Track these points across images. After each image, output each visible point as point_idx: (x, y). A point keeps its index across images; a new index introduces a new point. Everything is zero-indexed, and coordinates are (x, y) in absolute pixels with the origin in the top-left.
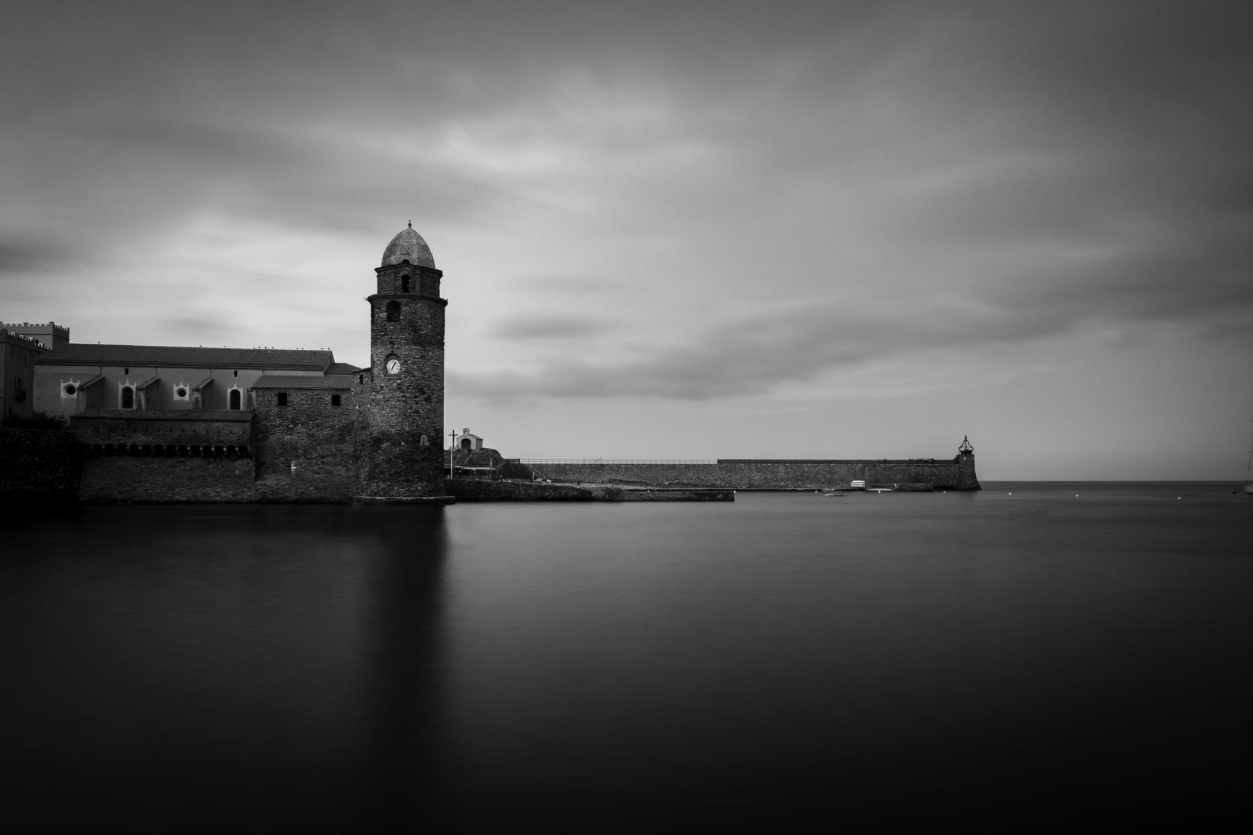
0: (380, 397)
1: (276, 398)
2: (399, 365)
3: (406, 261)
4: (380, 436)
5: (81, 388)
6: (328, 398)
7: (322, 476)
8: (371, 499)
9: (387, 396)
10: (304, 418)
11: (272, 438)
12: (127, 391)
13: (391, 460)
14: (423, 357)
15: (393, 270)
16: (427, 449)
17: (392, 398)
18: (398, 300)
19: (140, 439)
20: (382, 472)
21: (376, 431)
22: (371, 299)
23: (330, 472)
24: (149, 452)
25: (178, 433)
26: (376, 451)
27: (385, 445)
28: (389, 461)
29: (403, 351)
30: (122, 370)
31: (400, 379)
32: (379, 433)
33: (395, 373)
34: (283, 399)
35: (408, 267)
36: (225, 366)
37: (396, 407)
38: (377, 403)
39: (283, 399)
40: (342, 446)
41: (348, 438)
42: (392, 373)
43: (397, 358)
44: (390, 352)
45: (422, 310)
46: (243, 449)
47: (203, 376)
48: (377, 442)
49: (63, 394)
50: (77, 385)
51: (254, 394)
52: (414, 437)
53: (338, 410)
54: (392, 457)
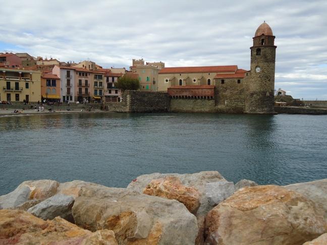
0: (253, 80)
1: (221, 81)
3: (263, 34)
5: (170, 80)
6: (237, 81)
10: (229, 87)
11: (220, 94)
14: (268, 66)
16: (268, 97)
18: (260, 48)
19: (184, 94)
22: (251, 48)
24: (187, 98)
27: (255, 96)
28: (256, 101)
29: (261, 64)
30: (179, 74)
34: (223, 82)
36: (207, 72)
39: (223, 82)
40: (240, 96)
43: (260, 67)
45: (268, 51)
47: (200, 75)
48: (252, 95)
49: (165, 82)
50: (168, 79)
51: (215, 80)
52: (264, 93)
53: (239, 84)
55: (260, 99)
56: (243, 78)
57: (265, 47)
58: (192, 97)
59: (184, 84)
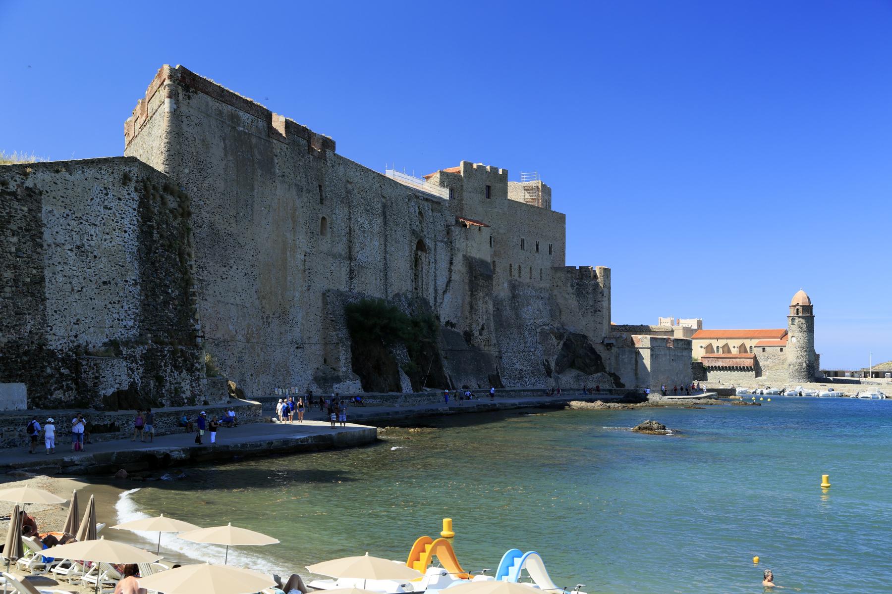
6: (779, 349)
7: (777, 376)
12: (718, 347)
19: (720, 363)
23: (779, 375)
25: (731, 362)
27: (792, 366)
34: (764, 350)
39: (764, 350)
46: (751, 367)
47: (739, 342)
48: (790, 365)
49: (700, 348)
53: (782, 353)
55: (797, 369)
56: (785, 346)
57: (799, 317)
58: (729, 367)
59: (721, 350)
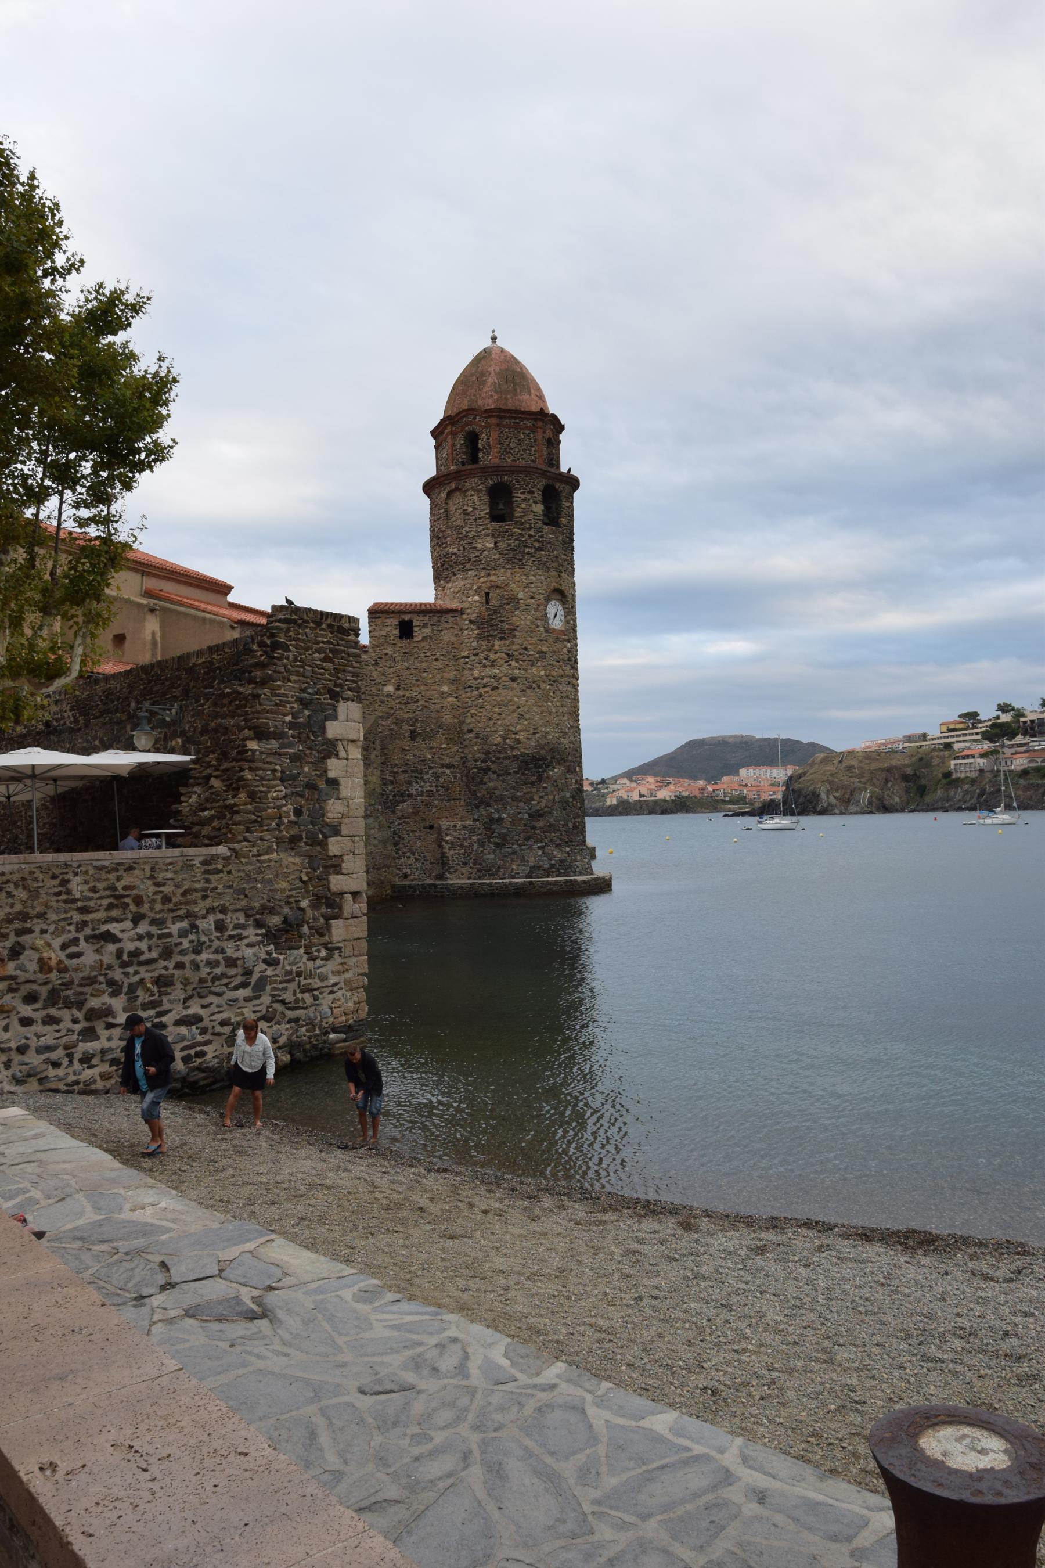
0: (537, 672)
2: (562, 612)
4: (543, 752)
8: (566, 882)
9: (555, 674)
13: (567, 802)
15: (540, 424)
17: (561, 677)
18: (558, 485)
20: (551, 829)
21: (533, 743)
26: (533, 784)
27: (557, 771)
31: (569, 641)
32: (539, 746)
33: (558, 627)
35: (553, 424)
37: (567, 697)
38: (533, 685)
41: (373, 756)
42: (553, 626)
44: (557, 586)
54: (568, 795)
